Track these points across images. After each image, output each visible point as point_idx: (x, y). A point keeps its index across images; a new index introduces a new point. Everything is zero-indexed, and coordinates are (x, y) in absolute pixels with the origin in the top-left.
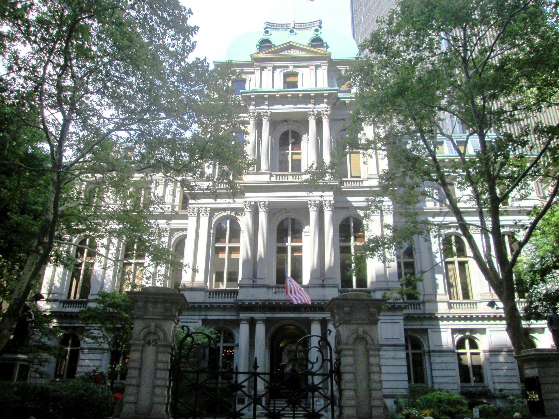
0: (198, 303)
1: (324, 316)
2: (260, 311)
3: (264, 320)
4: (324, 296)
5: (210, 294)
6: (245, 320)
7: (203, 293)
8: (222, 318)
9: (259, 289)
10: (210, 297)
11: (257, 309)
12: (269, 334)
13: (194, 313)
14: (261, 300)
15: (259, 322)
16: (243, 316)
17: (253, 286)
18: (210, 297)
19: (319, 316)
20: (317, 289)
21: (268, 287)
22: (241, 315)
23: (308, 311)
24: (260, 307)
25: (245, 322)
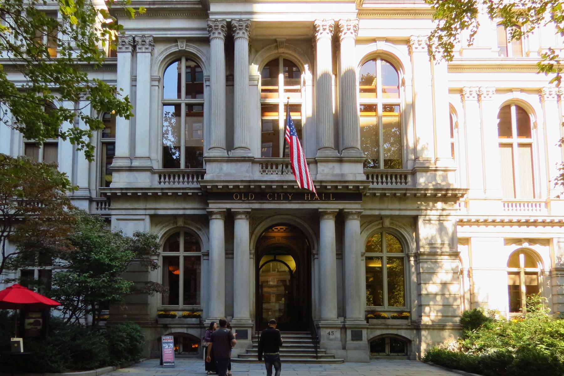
0: (142, 189)
1: (341, 206)
2: (240, 199)
3: (247, 212)
4: (342, 175)
5: (160, 178)
6: (220, 213)
7: (148, 174)
8: (181, 212)
9: (239, 164)
10: (160, 183)
11: (236, 197)
12: (254, 237)
13: (136, 206)
14: (242, 181)
15: (239, 217)
16: (214, 206)
17: (230, 160)
18: (160, 183)
19: (335, 206)
20: (331, 165)
21: (252, 161)
22: (211, 206)
23: (316, 199)
24: (240, 194)
25: (218, 216)
